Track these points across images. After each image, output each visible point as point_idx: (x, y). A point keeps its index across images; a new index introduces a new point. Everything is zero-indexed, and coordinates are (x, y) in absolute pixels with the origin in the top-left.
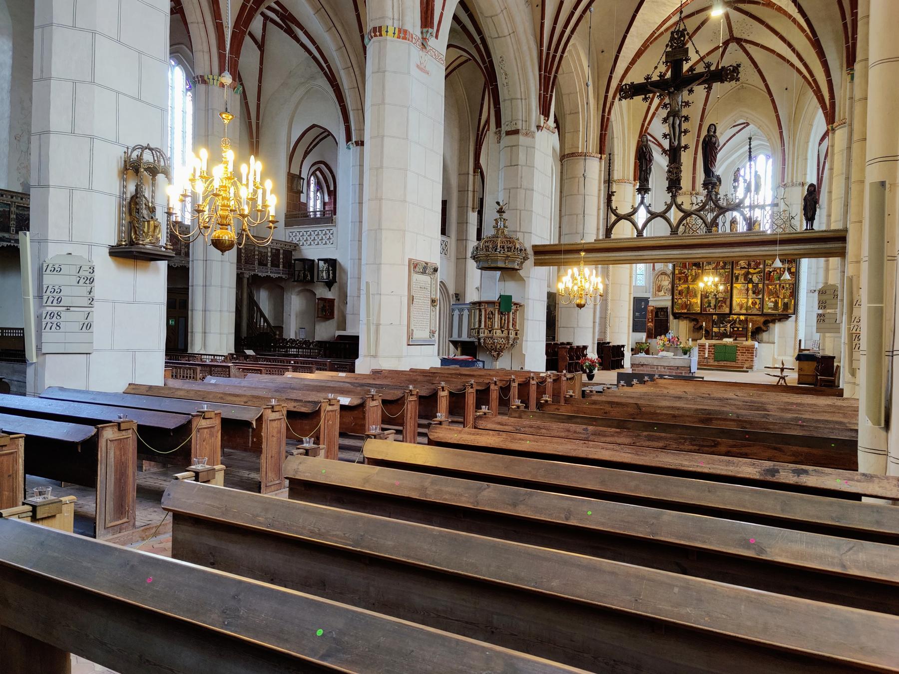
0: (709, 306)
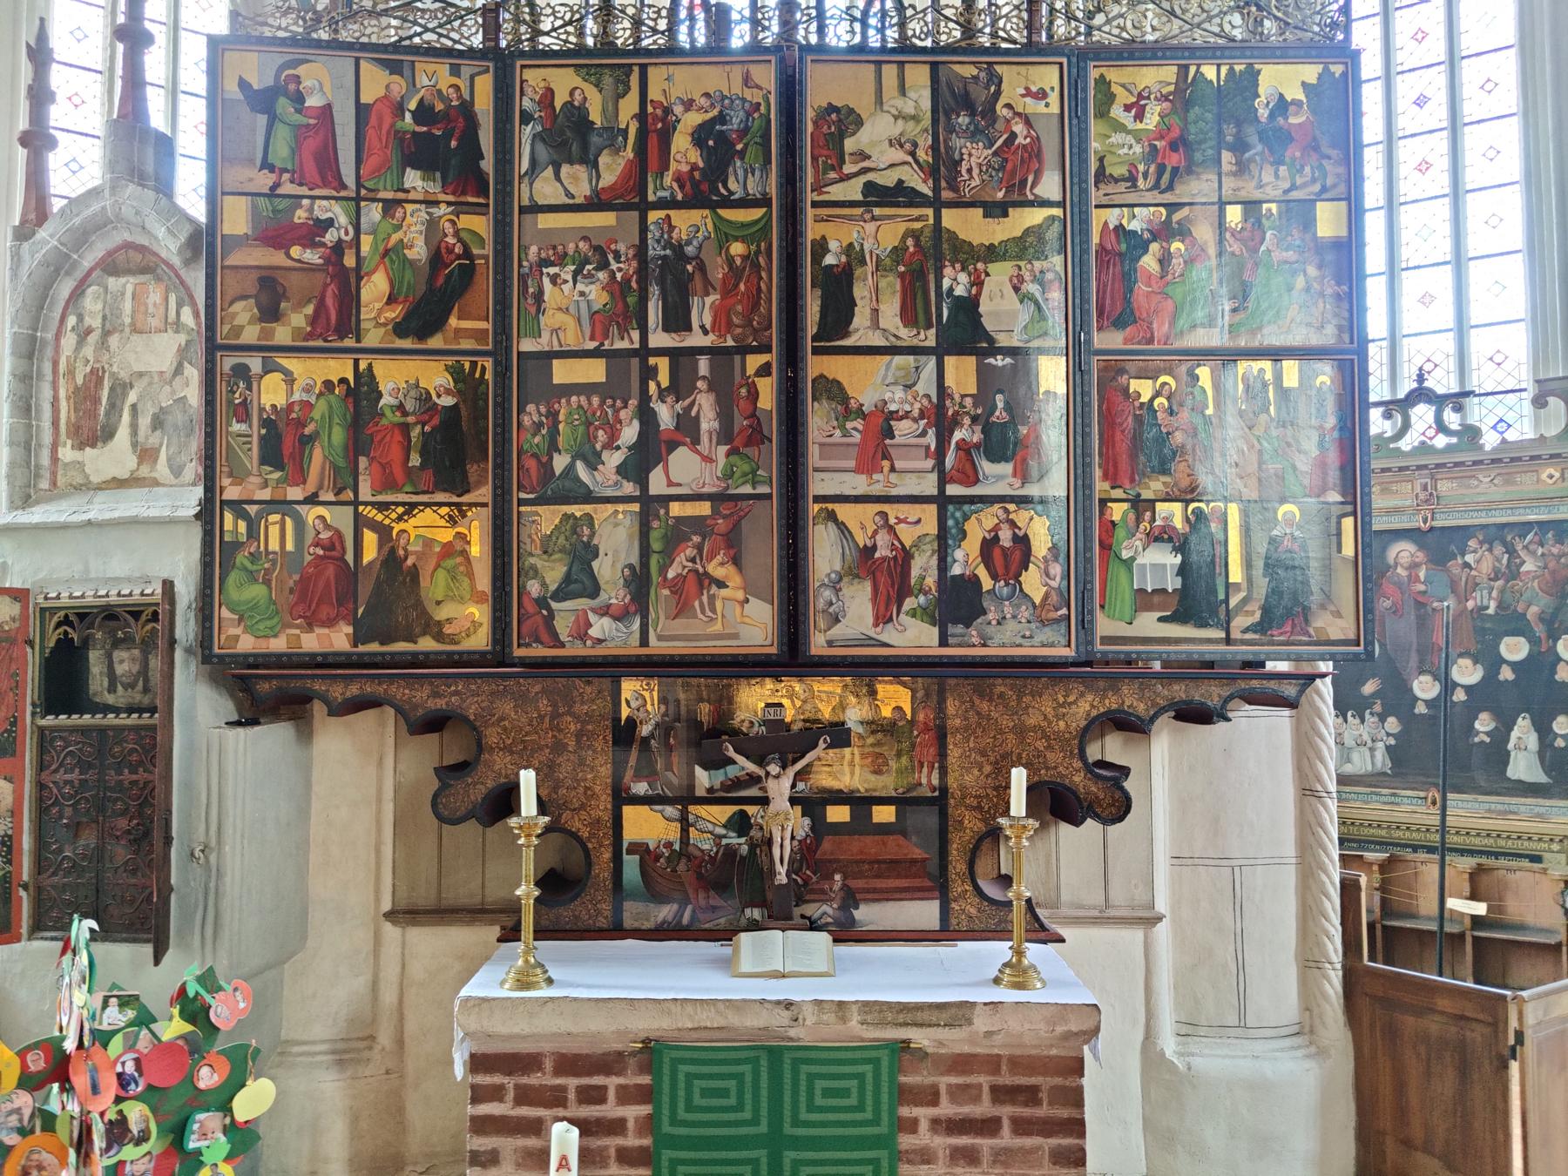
0: (581, 582)
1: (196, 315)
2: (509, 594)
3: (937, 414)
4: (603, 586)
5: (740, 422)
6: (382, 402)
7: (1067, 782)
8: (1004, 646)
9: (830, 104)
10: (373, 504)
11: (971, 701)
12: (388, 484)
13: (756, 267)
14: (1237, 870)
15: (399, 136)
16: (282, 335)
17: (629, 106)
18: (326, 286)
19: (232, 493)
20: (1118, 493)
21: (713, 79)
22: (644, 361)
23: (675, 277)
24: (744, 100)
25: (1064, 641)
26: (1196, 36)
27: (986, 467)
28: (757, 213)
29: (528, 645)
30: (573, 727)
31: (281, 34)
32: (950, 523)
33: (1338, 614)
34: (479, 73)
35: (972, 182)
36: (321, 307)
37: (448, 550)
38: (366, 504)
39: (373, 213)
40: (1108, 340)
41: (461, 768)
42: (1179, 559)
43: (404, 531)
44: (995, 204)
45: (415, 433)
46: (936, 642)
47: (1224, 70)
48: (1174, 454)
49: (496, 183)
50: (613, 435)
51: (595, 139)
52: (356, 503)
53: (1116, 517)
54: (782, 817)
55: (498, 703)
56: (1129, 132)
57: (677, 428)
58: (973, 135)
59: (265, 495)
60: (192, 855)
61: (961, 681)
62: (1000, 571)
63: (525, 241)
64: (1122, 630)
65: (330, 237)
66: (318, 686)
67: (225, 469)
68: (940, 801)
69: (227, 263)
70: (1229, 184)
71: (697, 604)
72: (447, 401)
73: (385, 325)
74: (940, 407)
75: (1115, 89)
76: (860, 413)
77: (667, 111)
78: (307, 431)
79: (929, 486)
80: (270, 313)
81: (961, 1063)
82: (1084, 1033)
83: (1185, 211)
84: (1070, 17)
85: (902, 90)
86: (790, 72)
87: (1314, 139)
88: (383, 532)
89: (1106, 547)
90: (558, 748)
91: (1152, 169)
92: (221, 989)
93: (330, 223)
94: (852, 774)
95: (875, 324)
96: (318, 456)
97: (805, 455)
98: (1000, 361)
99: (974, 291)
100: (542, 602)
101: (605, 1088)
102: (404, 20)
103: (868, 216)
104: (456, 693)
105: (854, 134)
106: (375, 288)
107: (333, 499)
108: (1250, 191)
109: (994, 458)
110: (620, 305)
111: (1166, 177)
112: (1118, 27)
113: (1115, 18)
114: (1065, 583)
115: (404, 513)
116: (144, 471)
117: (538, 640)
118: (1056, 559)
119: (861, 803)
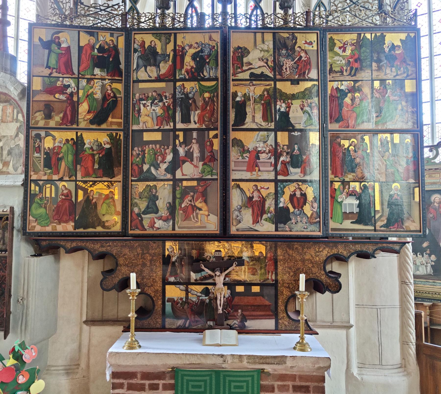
0: (152, 208)
1: (23, 116)
3: (275, 152)
4: (160, 209)
5: (207, 154)
7: (319, 279)
8: (297, 231)
9: (238, 46)
10: (82, 181)
11: (286, 250)
12: (87, 174)
13: (213, 101)
14: (379, 310)
15: (93, 57)
16: (52, 124)
17: (170, 47)
18: (67, 107)
19: (34, 177)
20: (337, 179)
21: (199, 38)
23: (185, 105)
24: (209, 45)
25: (318, 230)
26: (364, 23)
27: (292, 170)
28: (213, 83)
29: (134, 230)
30: (149, 258)
31: (53, 22)
32: (279, 189)
33: (413, 221)
35: (287, 73)
36: (65, 115)
37: (107, 197)
38: (79, 181)
39: (83, 83)
40: (333, 126)
41: (111, 271)
43: (92, 190)
44: (295, 80)
45: (96, 157)
46: (274, 230)
47: (373, 35)
48: (356, 165)
49: (125, 72)
50: (164, 158)
51: (159, 58)
52: (76, 181)
53: (336, 187)
54: (220, 290)
55: (123, 249)
56: (340, 56)
57: (186, 156)
59: (45, 178)
60: (18, 301)
61: (283, 243)
62: (296, 205)
63: (135, 91)
64: (338, 226)
65: (69, 91)
66: (62, 243)
67: (32, 169)
68: (275, 284)
69: (34, 99)
70: (375, 74)
71: (192, 216)
72: (108, 146)
73: (87, 120)
74: (276, 149)
75: (336, 41)
76: (248, 151)
77: (183, 48)
78: (60, 156)
79: (272, 176)
80: (48, 116)
81: (282, 377)
82: (325, 367)
83: (360, 83)
84: (320, 17)
85: (263, 42)
87: (404, 58)
88: (85, 191)
89: (333, 197)
90: (144, 265)
91: (349, 68)
92: (27, 348)
93: (69, 86)
94: (245, 275)
95: (254, 121)
96: (63, 164)
97: (229, 165)
98: (296, 134)
99: (287, 110)
100: (139, 215)
101: (158, 384)
102: (95, 18)
103: (251, 84)
104: (109, 246)
105: (247, 56)
106: (84, 108)
108: (382, 76)
109: (294, 166)
110: (167, 114)
111: (353, 71)
112: (337, 20)
113: (336, 17)
114: (318, 210)
115: (92, 184)
116: (5, 169)
117: (137, 228)
118: (316, 202)
119: (248, 285)
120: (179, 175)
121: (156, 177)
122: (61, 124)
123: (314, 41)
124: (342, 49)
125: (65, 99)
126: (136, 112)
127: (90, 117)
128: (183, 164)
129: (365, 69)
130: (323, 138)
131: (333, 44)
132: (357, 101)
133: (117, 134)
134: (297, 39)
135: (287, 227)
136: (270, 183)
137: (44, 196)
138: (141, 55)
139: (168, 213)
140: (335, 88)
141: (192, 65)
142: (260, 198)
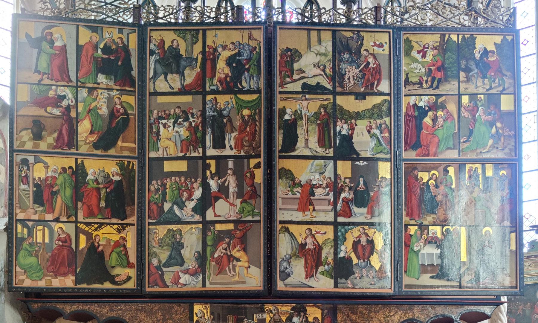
0: (176, 259)
2: (144, 264)
4: (185, 260)
5: (247, 188)
6: (88, 178)
10: (84, 223)
11: (348, 315)
12: (91, 214)
13: (254, 120)
15: (95, 59)
17: (198, 48)
18: (63, 125)
20: (413, 222)
21: (236, 36)
22: (204, 162)
23: (218, 125)
24: (249, 45)
27: (356, 210)
28: (255, 96)
29: (152, 287)
32: (339, 234)
34: (131, 33)
35: (350, 84)
37: (117, 244)
38: (81, 223)
39: (83, 93)
42: (439, 251)
43: (98, 235)
44: (360, 94)
45: (103, 192)
46: (332, 286)
47: (460, 36)
50: (191, 194)
51: (183, 63)
52: (76, 222)
53: (412, 233)
56: (419, 63)
57: (219, 191)
58: (351, 62)
59: (36, 217)
62: (361, 254)
65: (65, 103)
67: (18, 205)
70: (463, 86)
71: (227, 268)
72: (117, 178)
74: (335, 183)
75: (413, 43)
76: (300, 184)
77: (215, 50)
78: (54, 190)
79: (330, 217)
83: (444, 98)
85: (319, 42)
86: (270, 36)
87: (500, 67)
88: (89, 235)
89: (407, 246)
91: (430, 79)
93: (64, 97)
95: (307, 146)
96: (59, 200)
97: (275, 202)
98: (361, 163)
99: (350, 132)
100: (159, 268)
103: (304, 98)
105: (298, 61)
106: (84, 127)
107: (66, 220)
108: (472, 89)
109: (359, 206)
110: (194, 137)
112: (415, 19)
113: (413, 15)
115: (98, 228)
117: (157, 285)
120: (210, 215)
121: (181, 219)
122: (55, 147)
123: (386, 43)
124: (421, 54)
125: (60, 114)
126: (154, 135)
127: (93, 139)
128: (215, 202)
129: (450, 80)
130: (395, 170)
131: (410, 48)
132: (440, 121)
133: (129, 162)
134: (363, 39)
135: (349, 282)
136: (328, 226)
137: (34, 241)
138: (160, 58)
139: (197, 266)
140: (411, 105)
141: (226, 72)
142: (315, 245)
